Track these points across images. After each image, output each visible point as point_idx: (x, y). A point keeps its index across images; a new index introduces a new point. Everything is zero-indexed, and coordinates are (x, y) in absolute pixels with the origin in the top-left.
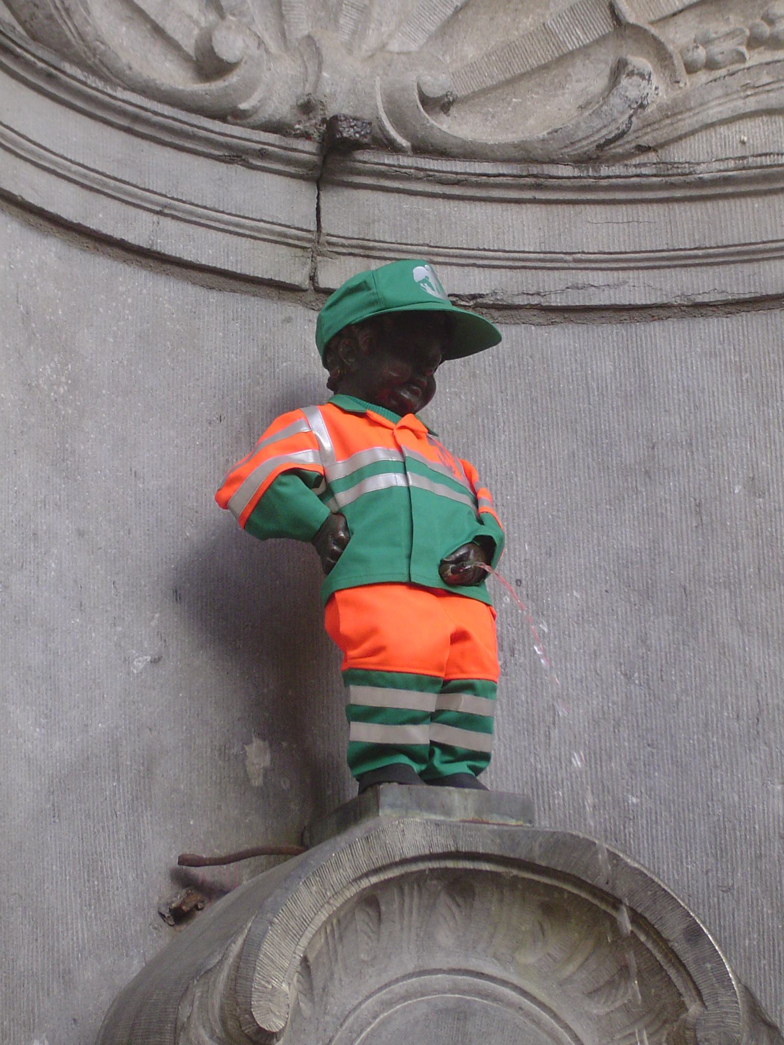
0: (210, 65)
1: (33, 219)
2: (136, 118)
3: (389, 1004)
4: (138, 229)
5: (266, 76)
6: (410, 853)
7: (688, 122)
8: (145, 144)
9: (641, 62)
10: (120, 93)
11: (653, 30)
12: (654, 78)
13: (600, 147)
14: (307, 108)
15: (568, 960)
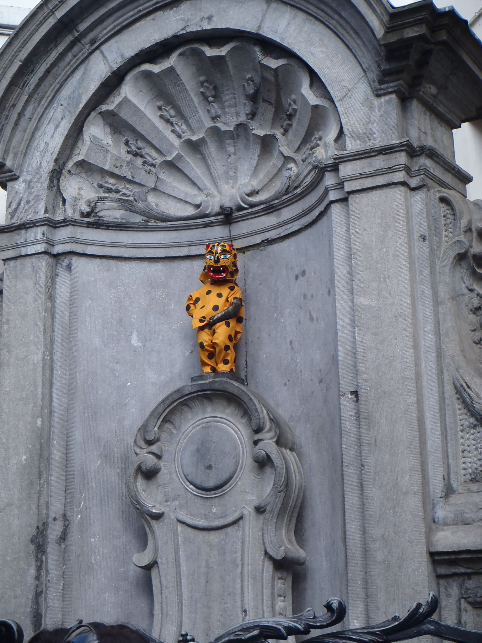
0: (198, 206)
1: (152, 260)
2: (176, 227)
3: (195, 427)
4: (184, 252)
5: (211, 203)
6: (187, 393)
7: (302, 177)
8: (182, 231)
9: (292, 165)
10: (169, 223)
11: (292, 155)
12: (293, 169)
13: (286, 191)
14: (221, 207)
15: (236, 410)
